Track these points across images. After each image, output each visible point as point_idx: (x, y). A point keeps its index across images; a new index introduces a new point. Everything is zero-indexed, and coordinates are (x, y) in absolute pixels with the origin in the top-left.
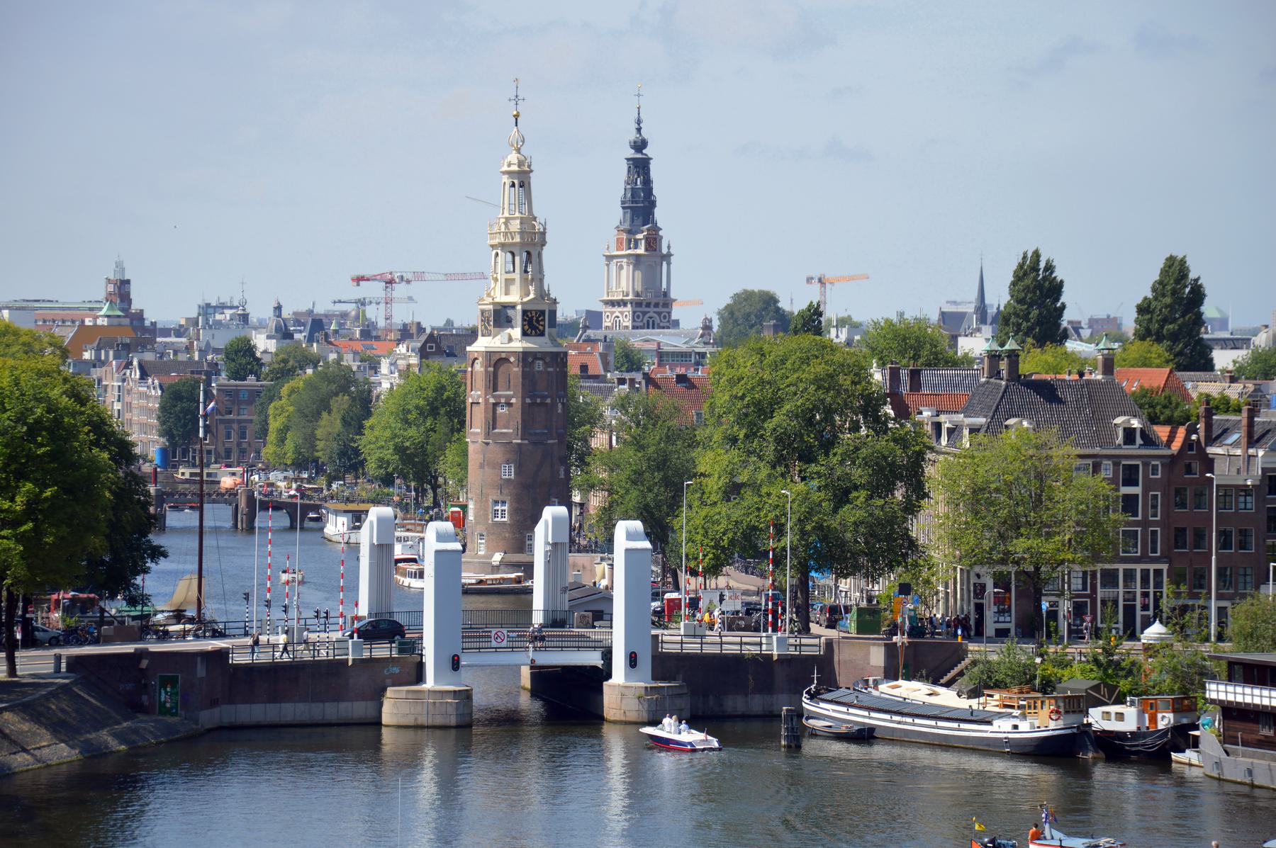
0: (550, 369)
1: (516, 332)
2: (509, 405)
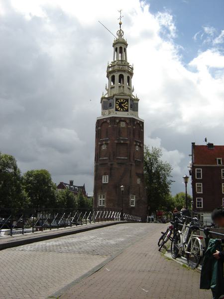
0: (129, 126)
1: (114, 109)
2: (107, 144)
